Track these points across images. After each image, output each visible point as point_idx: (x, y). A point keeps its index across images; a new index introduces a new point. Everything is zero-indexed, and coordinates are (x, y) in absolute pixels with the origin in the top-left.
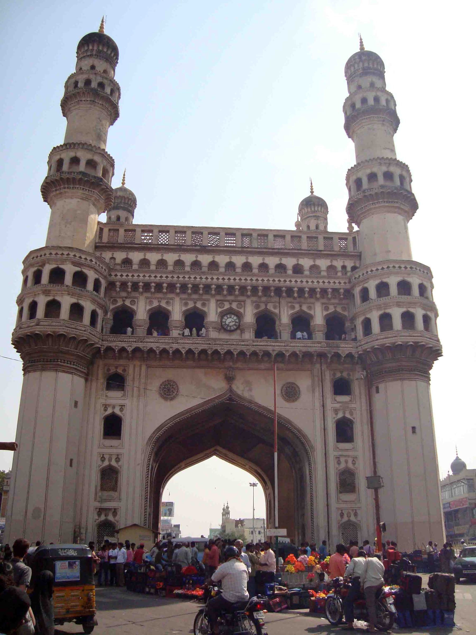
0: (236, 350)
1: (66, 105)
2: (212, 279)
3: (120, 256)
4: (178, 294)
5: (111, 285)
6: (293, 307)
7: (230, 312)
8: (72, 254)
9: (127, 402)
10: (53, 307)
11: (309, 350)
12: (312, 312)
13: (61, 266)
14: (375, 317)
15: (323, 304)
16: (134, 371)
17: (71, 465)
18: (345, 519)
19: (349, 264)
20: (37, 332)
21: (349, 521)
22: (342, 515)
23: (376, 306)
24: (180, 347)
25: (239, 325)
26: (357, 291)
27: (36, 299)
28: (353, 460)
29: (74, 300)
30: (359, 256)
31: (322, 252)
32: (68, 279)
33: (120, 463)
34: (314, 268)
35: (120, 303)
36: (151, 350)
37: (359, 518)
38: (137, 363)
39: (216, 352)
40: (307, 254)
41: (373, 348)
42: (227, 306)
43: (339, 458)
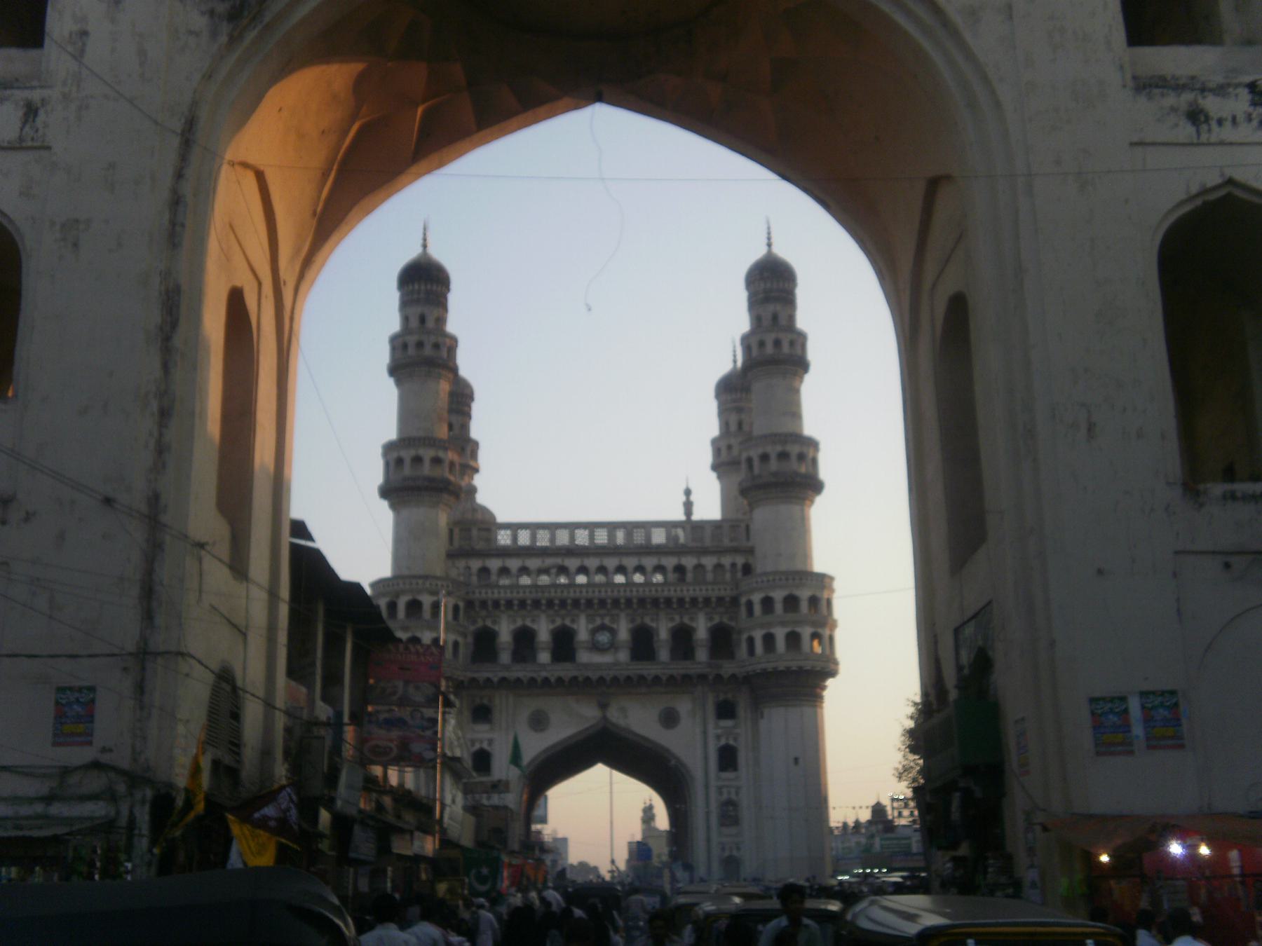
0: (608, 675)
1: (396, 370)
3: (476, 564)
5: (470, 604)
6: (672, 619)
7: (603, 628)
12: (694, 625)
16: (502, 703)
18: (727, 854)
26: (743, 600)
30: (750, 551)
34: (699, 567)
35: (480, 624)
36: (518, 680)
39: (588, 679)
42: (598, 622)
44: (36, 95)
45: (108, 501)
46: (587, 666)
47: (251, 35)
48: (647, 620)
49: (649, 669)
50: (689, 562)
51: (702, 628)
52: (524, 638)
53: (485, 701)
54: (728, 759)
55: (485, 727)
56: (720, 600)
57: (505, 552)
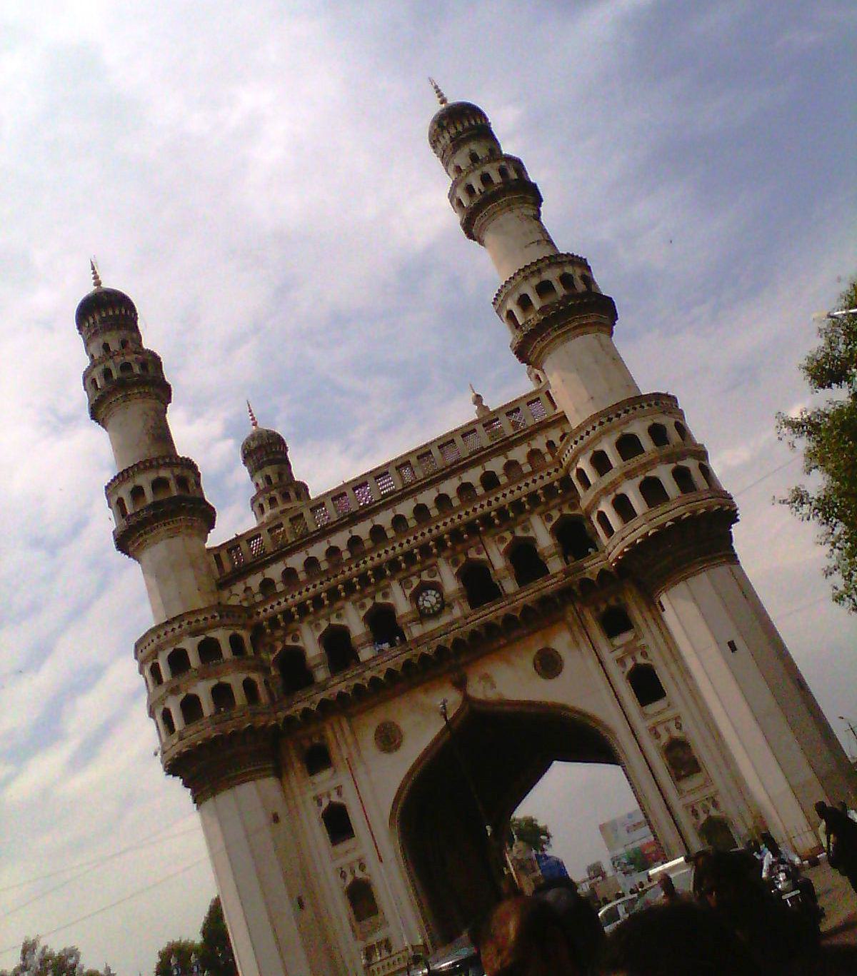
0: (447, 641)
2: (379, 556)
3: (254, 581)
4: (347, 598)
5: (257, 631)
6: (502, 540)
7: (424, 587)
8: (185, 624)
9: (344, 778)
11: (544, 594)
12: (531, 534)
13: (179, 646)
14: (606, 507)
15: (540, 514)
17: (301, 905)
18: (703, 817)
19: (554, 435)
20: (184, 750)
21: (710, 818)
23: (602, 490)
24: (374, 673)
25: (442, 599)
26: (573, 474)
27: (167, 706)
28: (677, 723)
29: (214, 682)
30: (563, 419)
31: (510, 439)
33: (367, 870)
34: (511, 466)
37: (722, 806)
39: (424, 657)
41: (622, 553)
42: (415, 582)
43: (654, 727)
48: (473, 554)
49: (492, 613)
50: (496, 465)
51: (541, 533)
53: (316, 741)
54: (646, 685)
56: (549, 489)
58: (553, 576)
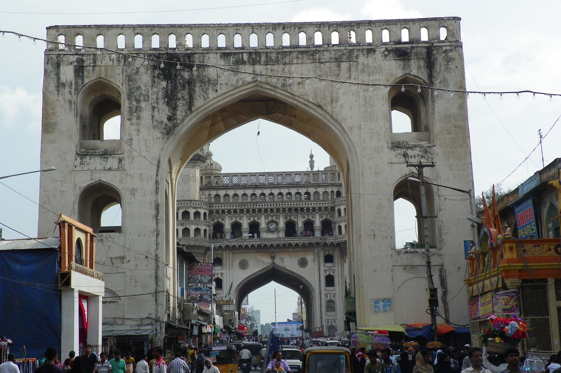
0: (275, 243)
3: (213, 193)
4: (245, 214)
5: (211, 212)
6: (304, 217)
7: (272, 221)
10: (186, 231)
12: (314, 220)
18: (330, 324)
22: (328, 322)
26: (337, 208)
32: (192, 216)
34: (316, 192)
35: (216, 220)
37: (336, 323)
38: (228, 252)
40: (313, 186)
44: (121, 156)
45: (147, 257)
46: (265, 239)
47: (172, 138)
48: (293, 218)
50: (312, 190)
52: (236, 227)
53: (219, 256)
54: (330, 281)
55: (220, 268)
56: (326, 208)
57: (226, 187)
58: (317, 238)
